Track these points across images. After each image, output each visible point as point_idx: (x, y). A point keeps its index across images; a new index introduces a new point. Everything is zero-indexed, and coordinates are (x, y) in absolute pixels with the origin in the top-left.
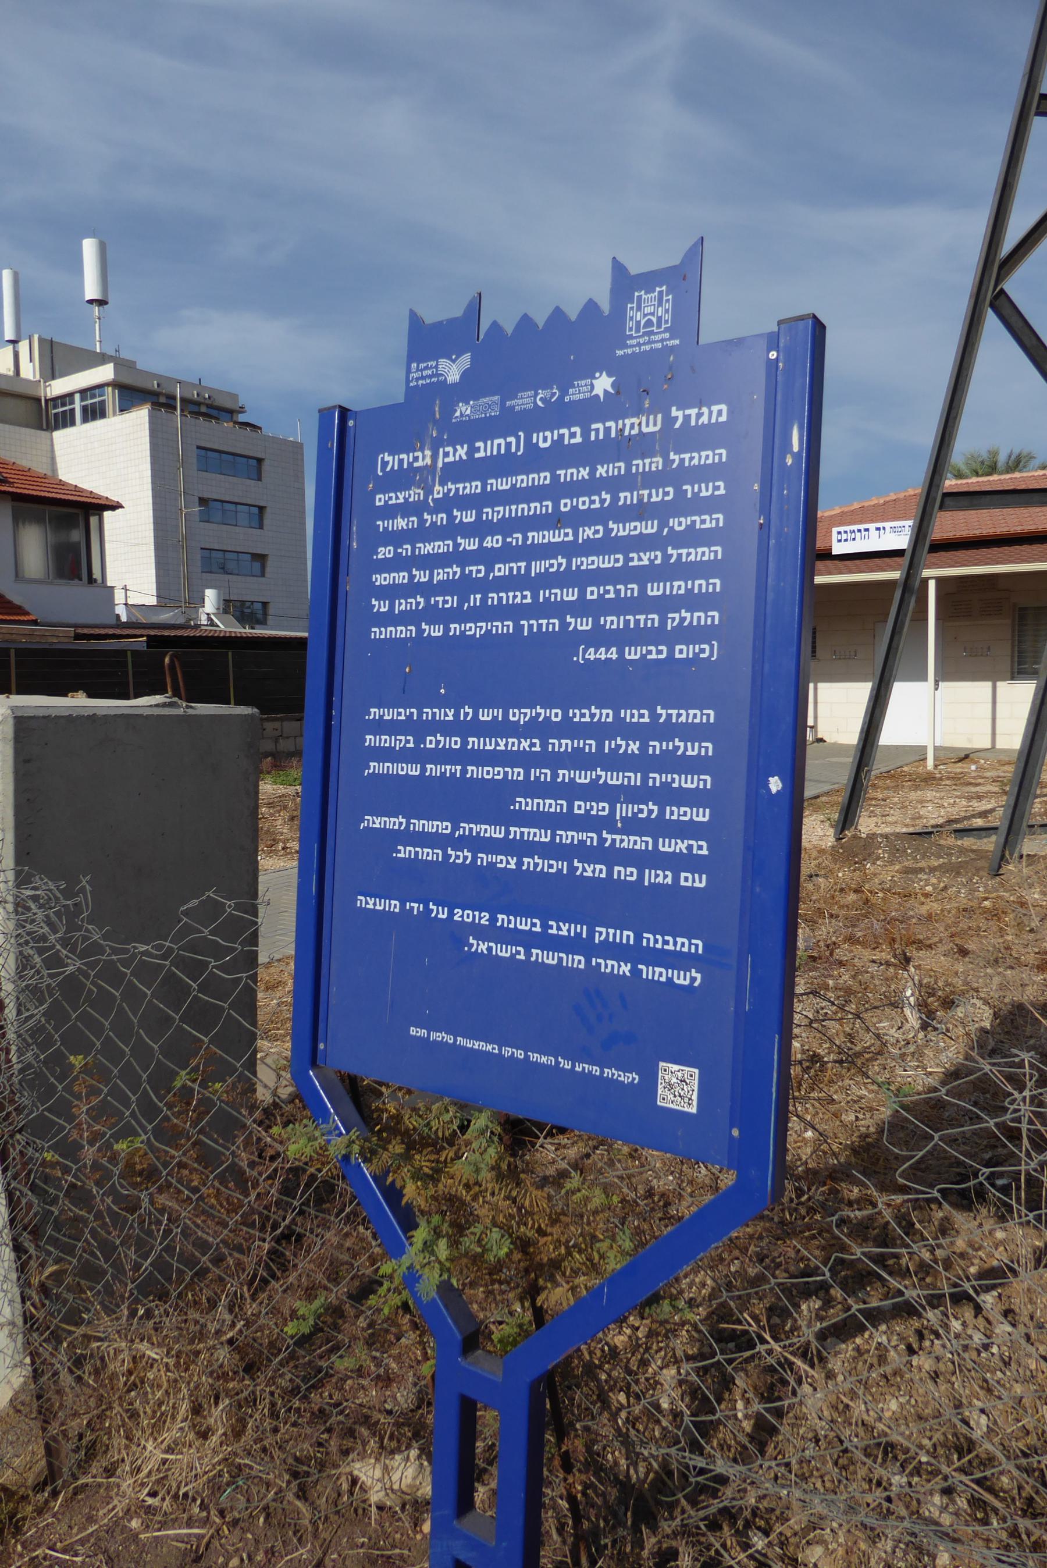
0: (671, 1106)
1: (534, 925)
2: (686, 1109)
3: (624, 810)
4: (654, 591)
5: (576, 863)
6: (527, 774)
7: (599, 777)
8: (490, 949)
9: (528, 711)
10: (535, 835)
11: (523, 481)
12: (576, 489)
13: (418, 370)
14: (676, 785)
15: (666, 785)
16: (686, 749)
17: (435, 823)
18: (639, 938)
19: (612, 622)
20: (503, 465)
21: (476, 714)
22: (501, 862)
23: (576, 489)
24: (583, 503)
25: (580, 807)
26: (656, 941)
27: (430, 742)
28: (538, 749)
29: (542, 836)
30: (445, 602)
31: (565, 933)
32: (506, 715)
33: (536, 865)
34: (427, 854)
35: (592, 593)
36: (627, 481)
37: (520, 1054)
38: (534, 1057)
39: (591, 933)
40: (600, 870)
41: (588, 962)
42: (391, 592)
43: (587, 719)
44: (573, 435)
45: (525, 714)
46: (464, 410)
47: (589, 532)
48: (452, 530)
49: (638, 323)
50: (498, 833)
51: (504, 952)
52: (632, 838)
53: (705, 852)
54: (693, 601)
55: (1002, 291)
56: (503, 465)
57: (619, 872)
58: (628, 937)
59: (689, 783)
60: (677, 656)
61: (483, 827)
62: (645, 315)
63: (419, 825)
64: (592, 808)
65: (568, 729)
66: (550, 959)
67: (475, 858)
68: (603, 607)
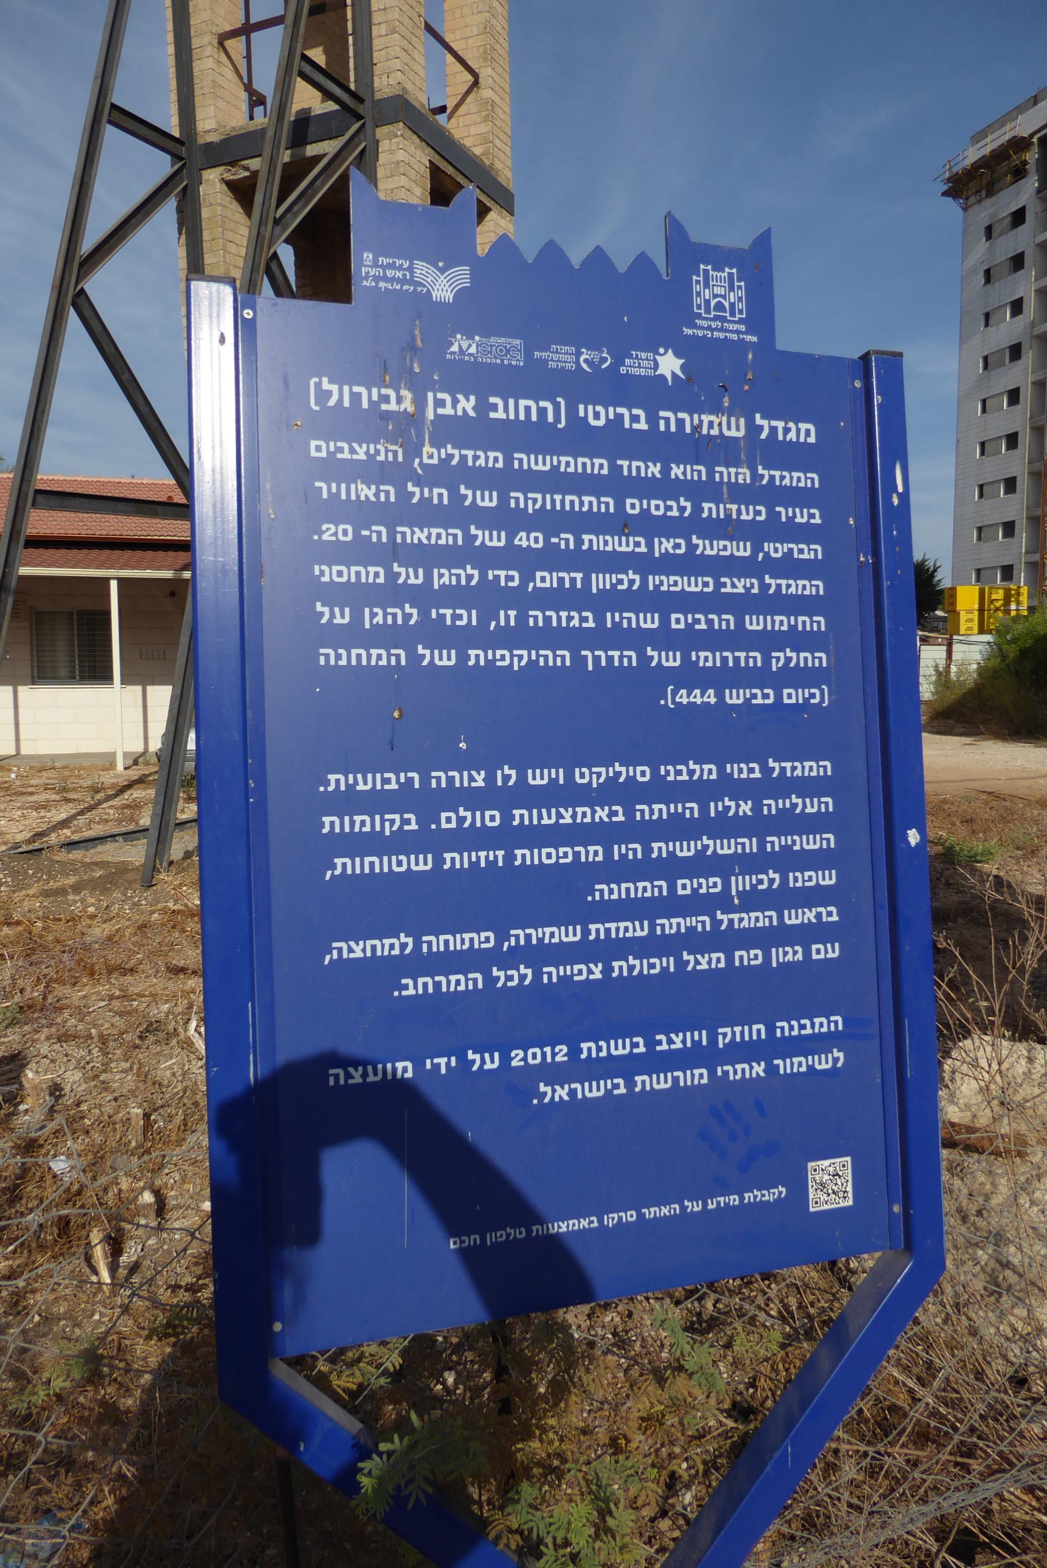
0: (826, 1207)
1: (635, 1045)
2: (842, 1205)
3: (740, 883)
4: (754, 624)
5: (686, 956)
6: (608, 853)
7: (706, 847)
8: (572, 1093)
9: (603, 770)
10: (626, 929)
11: (569, 464)
12: (646, 488)
13: (375, 264)
14: (797, 848)
15: (786, 849)
16: (805, 806)
17: (467, 936)
18: (771, 1029)
19: (706, 658)
21: (522, 777)
22: (580, 972)
23: (646, 488)
24: (657, 507)
25: (684, 887)
26: (791, 1028)
27: (447, 820)
28: (621, 818)
29: (638, 930)
30: (456, 617)
31: (679, 1045)
32: (569, 776)
33: (631, 968)
34: (456, 982)
35: (678, 621)
36: (710, 490)
37: (631, 1216)
38: (651, 1212)
39: (713, 1038)
40: (717, 960)
41: (712, 1073)
42: (356, 596)
43: (685, 777)
44: (635, 419)
45: (599, 774)
47: (667, 545)
48: (457, 514)
49: (707, 302)
50: (572, 936)
51: (594, 1091)
52: (753, 915)
53: (835, 918)
54: (798, 640)
55: (82, 290)
57: (741, 958)
58: (759, 1031)
59: (811, 843)
60: (786, 701)
61: (548, 930)
62: (715, 296)
63: (437, 943)
64: (700, 885)
65: (661, 790)
66: (662, 1083)
67: (538, 975)
68: (689, 640)
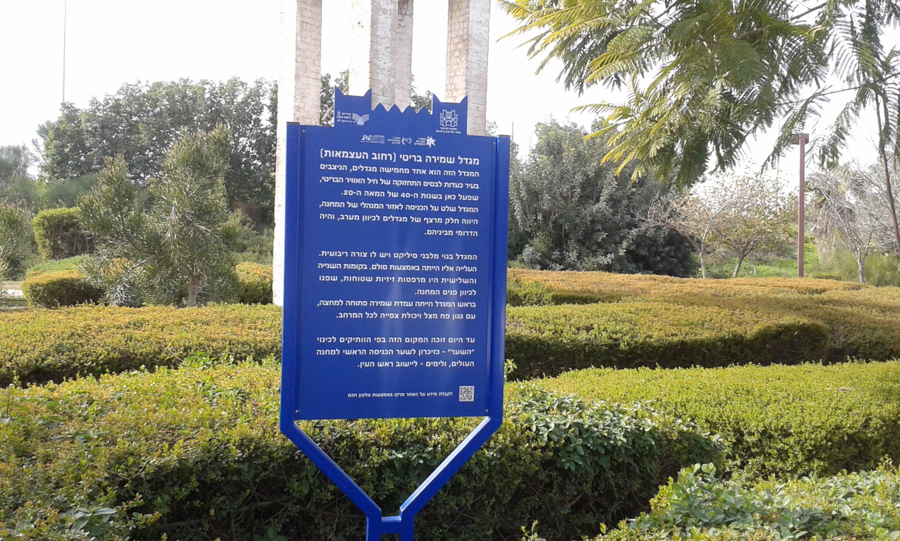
11: (397, 170)
20: (387, 163)
34: (355, 315)
37: (403, 395)
38: (409, 394)
44: (418, 159)
46: (366, 138)
56: (387, 163)
63: (350, 303)
